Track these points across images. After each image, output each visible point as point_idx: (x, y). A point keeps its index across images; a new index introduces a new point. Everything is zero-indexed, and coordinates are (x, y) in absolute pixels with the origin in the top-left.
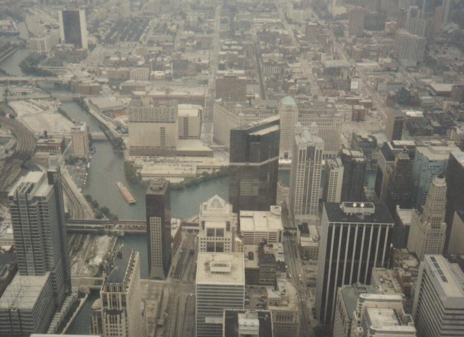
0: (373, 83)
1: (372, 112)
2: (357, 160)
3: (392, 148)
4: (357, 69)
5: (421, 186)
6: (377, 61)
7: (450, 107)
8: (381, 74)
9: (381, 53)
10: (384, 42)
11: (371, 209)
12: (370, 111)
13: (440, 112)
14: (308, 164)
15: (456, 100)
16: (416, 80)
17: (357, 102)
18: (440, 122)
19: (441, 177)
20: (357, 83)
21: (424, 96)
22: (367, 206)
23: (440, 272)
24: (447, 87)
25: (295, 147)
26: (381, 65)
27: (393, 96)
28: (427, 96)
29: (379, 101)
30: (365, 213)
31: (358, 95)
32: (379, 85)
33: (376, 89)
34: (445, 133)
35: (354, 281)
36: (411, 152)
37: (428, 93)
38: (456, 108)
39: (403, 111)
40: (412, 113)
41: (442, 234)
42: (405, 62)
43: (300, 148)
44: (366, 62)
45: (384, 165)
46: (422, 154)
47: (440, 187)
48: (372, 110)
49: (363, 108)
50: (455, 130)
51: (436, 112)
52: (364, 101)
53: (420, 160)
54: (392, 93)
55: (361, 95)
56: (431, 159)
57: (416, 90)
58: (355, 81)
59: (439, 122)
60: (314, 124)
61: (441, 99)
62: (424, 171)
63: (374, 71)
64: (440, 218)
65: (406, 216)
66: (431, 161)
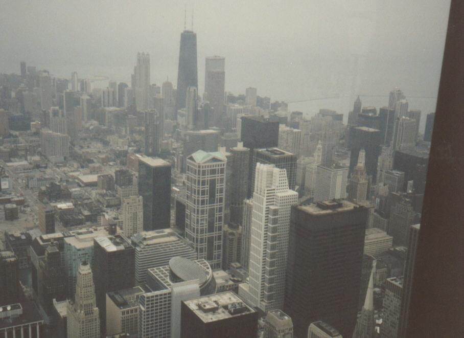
0: (24, 181)
1: (26, 209)
2: (8, 260)
3: (41, 243)
4: (6, 169)
5: (74, 276)
6: (26, 159)
7: (98, 196)
8: (31, 172)
9: (30, 151)
10: (32, 142)
11: (18, 310)
12: (22, 208)
13: (90, 201)
15: (103, 188)
16: (65, 174)
17: (9, 201)
18: (90, 210)
19: (85, 264)
20: (7, 183)
21: (73, 188)
24: (93, 178)
26: (30, 163)
27: (44, 191)
28: (76, 188)
29: (32, 198)
30: (12, 315)
31: (10, 194)
32: (30, 182)
33: (27, 186)
34: (96, 221)
36: (61, 244)
37: (76, 185)
38: (103, 195)
39: (52, 204)
40: (63, 205)
41: (96, 319)
42: (53, 159)
44: (16, 162)
45: (38, 261)
46: (70, 245)
47: (86, 274)
48: (24, 207)
49: (15, 206)
50: (104, 215)
51: (86, 201)
52: (16, 199)
53: (69, 250)
54: (43, 188)
55: (13, 194)
56: (78, 247)
57: (65, 184)
58: (6, 180)
59: (88, 211)
61: (89, 189)
62: (74, 260)
63: (24, 170)
64: (91, 304)
65: (62, 308)
66: (79, 250)
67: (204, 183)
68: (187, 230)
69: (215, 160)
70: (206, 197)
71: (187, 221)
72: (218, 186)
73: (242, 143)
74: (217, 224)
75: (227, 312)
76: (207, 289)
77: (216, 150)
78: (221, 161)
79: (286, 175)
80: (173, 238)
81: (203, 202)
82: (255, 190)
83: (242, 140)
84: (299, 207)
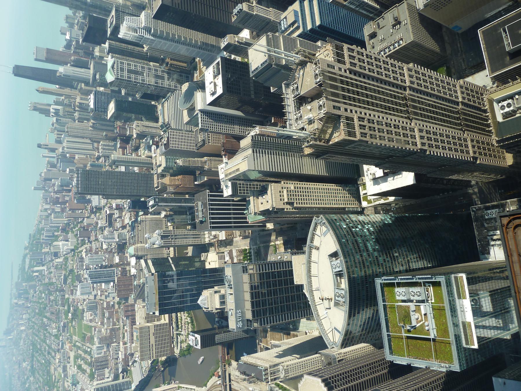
14: (172, 239)
22: (197, 206)
23: (234, 172)
25: (162, 247)
35: (244, 214)
43: (162, 245)
60: (146, 236)
67: (129, 77)
68: (161, 94)
69: (113, 67)
70: (140, 77)
71: (155, 93)
72: (133, 68)
73: (103, 45)
74: (160, 73)
75: (217, 77)
76: (201, 86)
77: (106, 65)
78: (114, 63)
79: (129, 17)
80: (166, 105)
81: (143, 80)
82: (138, 42)
83: (100, 45)
84: (154, 13)
